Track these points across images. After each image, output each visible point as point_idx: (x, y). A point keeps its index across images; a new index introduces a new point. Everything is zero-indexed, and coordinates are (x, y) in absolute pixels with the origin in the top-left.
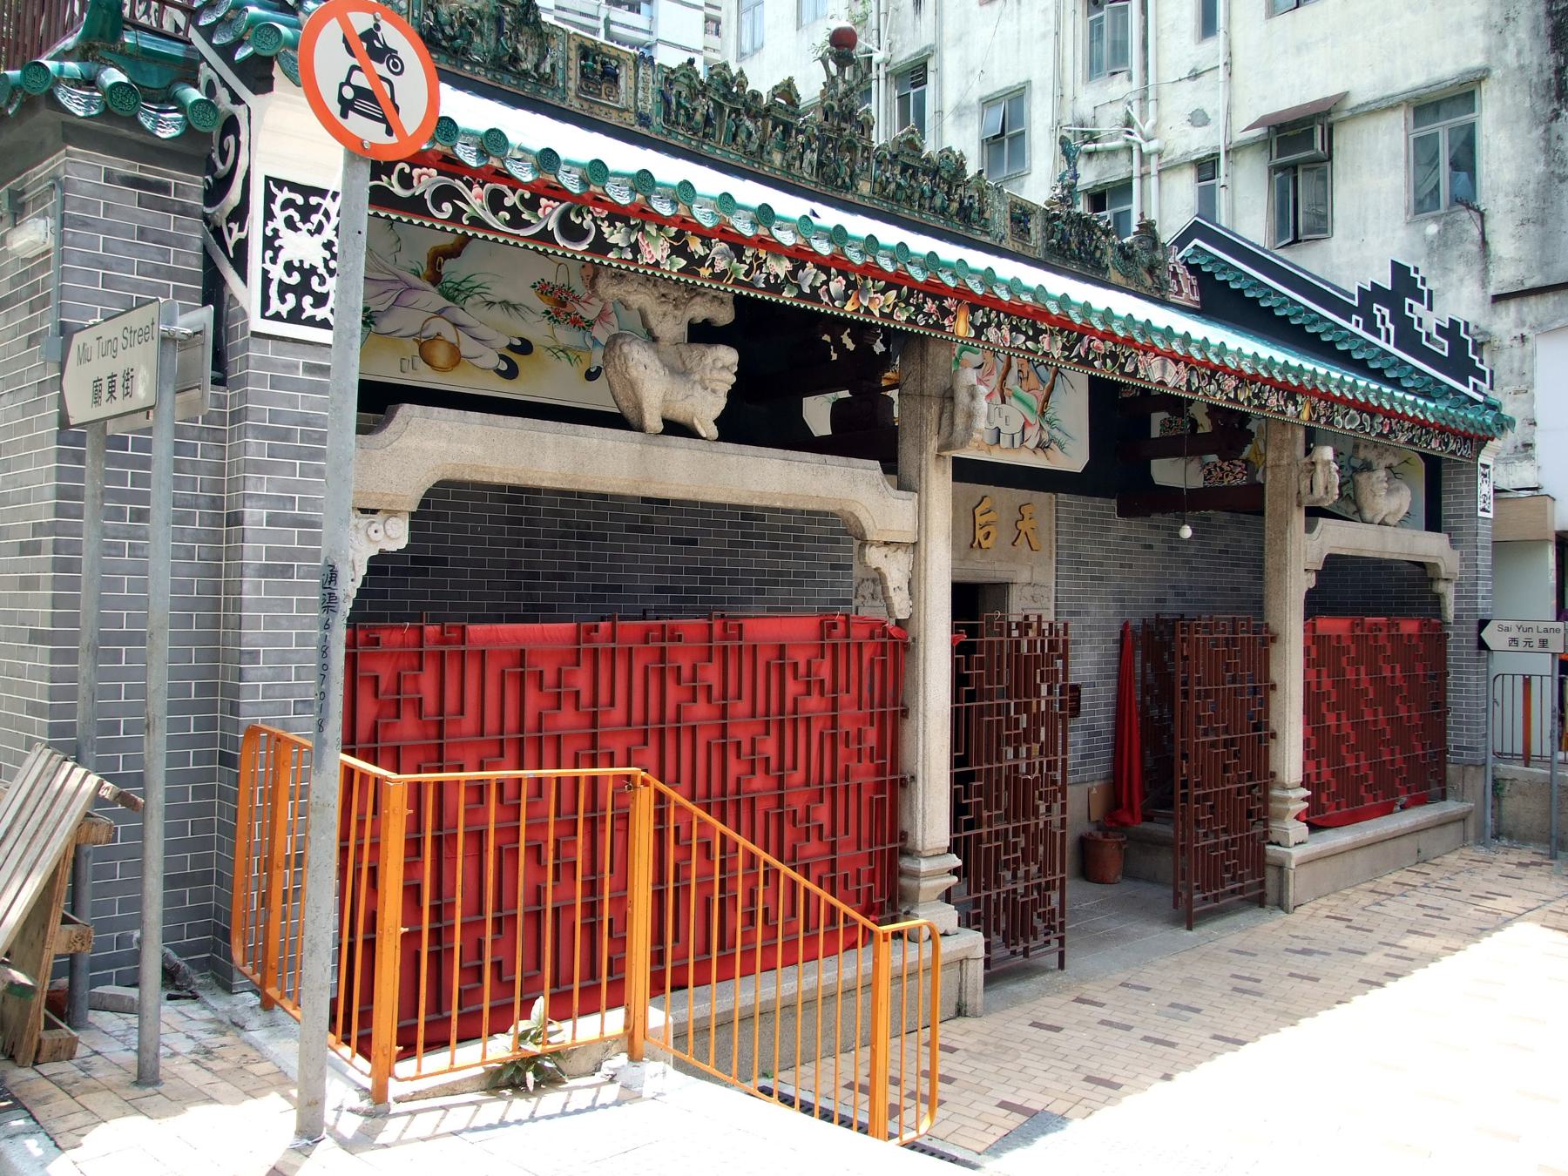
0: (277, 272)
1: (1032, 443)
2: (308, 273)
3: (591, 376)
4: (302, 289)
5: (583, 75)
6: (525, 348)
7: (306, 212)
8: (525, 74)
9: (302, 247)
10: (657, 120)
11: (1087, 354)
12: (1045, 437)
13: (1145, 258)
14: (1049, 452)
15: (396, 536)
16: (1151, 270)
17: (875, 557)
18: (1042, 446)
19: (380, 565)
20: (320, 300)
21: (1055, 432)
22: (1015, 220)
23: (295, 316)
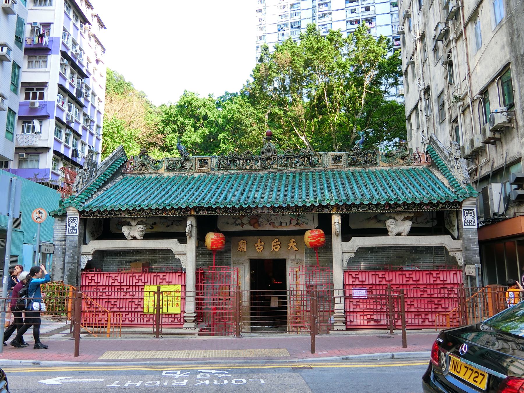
0: (70, 228)
1: (294, 224)
2: (73, 227)
3: (167, 226)
4: (72, 230)
5: (200, 165)
6: (155, 224)
7: (73, 220)
8: (186, 169)
9: (73, 224)
10: (216, 169)
11: (233, 211)
12: (300, 222)
13: (399, 155)
14: (301, 225)
15: (91, 258)
16: (403, 158)
17: (177, 257)
18: (298, 224)
19: (89, 262)
20: (75, 230)
21: (304, 220)
22: (334, 159)
23: (72, 233)
